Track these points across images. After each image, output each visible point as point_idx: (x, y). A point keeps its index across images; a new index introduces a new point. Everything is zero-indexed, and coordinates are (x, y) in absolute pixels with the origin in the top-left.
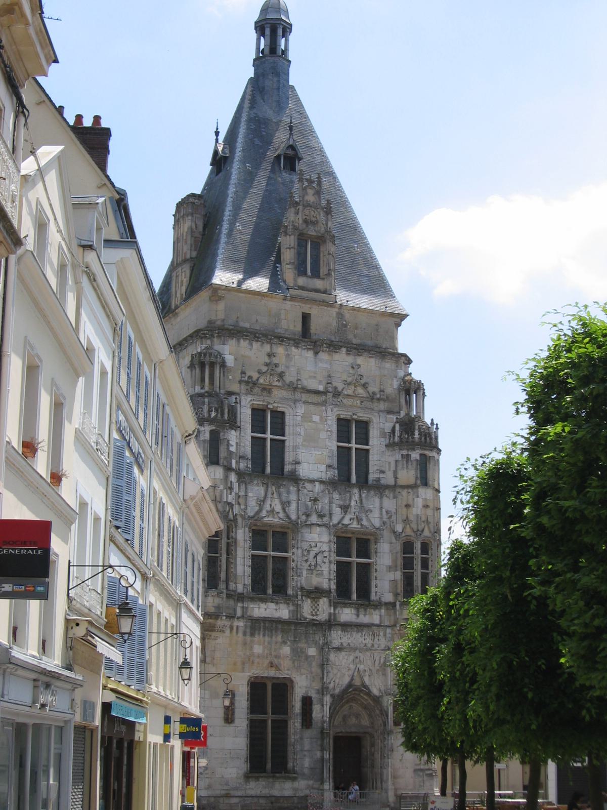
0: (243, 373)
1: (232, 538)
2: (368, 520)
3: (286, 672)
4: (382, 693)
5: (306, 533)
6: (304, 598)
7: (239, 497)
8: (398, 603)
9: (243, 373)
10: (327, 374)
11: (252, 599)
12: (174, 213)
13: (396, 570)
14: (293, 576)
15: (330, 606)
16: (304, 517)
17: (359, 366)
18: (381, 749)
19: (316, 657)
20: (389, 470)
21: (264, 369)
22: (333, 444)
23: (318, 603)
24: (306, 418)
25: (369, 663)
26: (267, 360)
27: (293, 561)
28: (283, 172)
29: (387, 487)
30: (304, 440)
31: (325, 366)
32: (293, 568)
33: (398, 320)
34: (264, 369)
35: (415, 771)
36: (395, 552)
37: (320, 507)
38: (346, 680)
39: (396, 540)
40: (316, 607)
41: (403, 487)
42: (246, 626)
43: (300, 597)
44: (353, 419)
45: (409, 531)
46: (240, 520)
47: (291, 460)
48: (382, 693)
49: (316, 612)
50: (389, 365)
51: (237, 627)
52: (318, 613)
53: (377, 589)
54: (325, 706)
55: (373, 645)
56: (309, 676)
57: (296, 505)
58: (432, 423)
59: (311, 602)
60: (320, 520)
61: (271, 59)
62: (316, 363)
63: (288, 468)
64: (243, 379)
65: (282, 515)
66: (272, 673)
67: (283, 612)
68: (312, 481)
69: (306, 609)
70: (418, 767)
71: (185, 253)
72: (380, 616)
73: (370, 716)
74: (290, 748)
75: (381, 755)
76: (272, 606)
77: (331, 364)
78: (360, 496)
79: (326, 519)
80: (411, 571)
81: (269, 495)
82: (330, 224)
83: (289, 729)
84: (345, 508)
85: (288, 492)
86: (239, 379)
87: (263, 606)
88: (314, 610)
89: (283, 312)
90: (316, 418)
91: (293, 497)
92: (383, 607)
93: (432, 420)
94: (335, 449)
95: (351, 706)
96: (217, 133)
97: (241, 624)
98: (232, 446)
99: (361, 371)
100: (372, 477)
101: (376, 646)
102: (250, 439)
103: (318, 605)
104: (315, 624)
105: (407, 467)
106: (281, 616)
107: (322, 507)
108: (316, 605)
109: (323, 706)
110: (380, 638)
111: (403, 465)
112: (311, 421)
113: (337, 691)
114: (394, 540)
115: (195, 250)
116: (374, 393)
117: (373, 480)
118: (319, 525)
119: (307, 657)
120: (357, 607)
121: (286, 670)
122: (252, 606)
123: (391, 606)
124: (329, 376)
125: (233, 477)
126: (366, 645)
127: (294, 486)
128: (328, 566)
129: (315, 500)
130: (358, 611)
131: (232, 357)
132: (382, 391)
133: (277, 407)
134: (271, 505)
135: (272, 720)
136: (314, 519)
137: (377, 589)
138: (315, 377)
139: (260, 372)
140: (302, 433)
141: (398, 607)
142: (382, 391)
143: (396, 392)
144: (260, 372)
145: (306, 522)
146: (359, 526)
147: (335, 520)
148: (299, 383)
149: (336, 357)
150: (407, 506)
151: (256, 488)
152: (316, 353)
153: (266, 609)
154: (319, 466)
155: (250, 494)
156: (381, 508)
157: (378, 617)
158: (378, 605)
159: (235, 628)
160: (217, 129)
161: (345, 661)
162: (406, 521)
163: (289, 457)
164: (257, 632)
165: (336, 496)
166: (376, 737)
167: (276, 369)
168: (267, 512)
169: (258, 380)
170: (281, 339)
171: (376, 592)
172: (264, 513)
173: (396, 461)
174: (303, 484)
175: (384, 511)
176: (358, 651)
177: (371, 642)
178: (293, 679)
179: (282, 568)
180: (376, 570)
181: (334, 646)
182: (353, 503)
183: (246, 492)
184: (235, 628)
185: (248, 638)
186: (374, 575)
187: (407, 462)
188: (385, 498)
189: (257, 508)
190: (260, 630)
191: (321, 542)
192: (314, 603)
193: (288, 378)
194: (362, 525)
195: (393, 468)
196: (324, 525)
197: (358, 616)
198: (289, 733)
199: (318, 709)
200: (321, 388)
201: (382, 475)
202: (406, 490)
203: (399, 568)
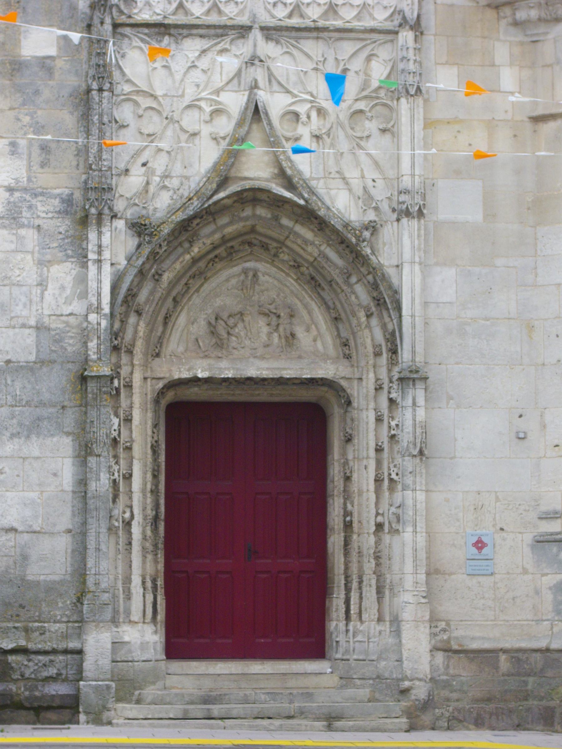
4: (376, 209)
18: (379, 450)
19: (60, 63)
48: (376, 209)
54: (92, 269)
56: (22, 143)
75: (378, 481)
95: (245, 272)
109: (84, 265)
161: (196, 76)
176: (256, 34)
181: (145, 16)
199: (68, 281)
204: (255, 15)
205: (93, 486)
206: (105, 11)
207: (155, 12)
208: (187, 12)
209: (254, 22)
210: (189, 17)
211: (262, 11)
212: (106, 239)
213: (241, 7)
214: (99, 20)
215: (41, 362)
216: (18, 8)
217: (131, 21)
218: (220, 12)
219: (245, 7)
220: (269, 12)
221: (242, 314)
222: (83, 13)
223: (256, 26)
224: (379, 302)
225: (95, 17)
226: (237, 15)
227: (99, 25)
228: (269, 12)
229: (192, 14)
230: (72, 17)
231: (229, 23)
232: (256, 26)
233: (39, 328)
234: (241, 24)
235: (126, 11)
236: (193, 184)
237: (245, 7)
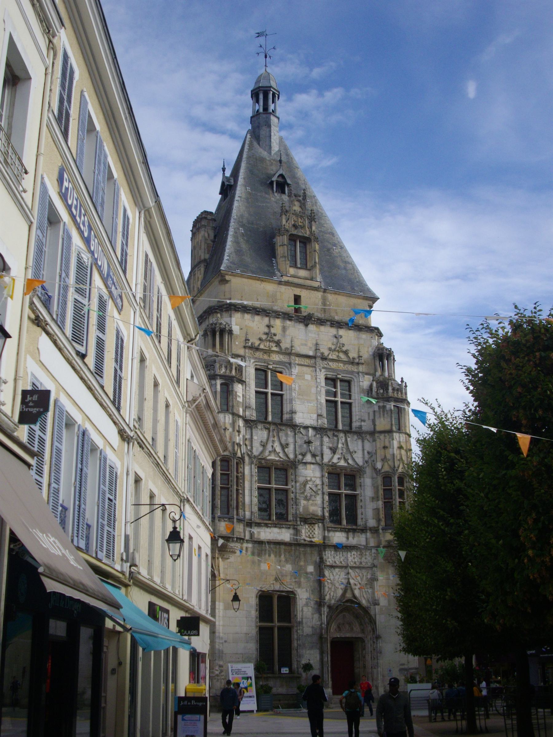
0: (247, 340)
1: (241, 472)
2: (354, 460)
3: (289, 586)
6: (302, 524)
7: (246, 439)
8: (380, 527)
9: (247, 340)
10: (315, 342)
11: (258, 525)
12: (191, 229)
13: (378, 500)
16: (300, 457)
17: (341, 337)
20: (369, 419)
21: (264, 337)
22: (323, 399)
24: (300, 376)
25: (359, 578)
26: (266, 330)
27: (293, 493)
28: (276, 194)
29: (367, 433)
30: (299, 395)
31: (313, 335)
32: (292, 499)
33: (371, 303)
34: (264, 337)
35: (401, 670)
36: (376, 485)
38: (340, 592)
39: (377, 475)
41: (381, 432)
42: (254, 547)
43: (299, 523)
44: (338, 378)
45: (386, 468)
46: (247, 459)
47: (288, 410)
50: (364, 336)
51: (247, 548)
52: (315, 536)
53: (363, 516)
55: (361, 563)
58: (402, 381)
59: (309, 527)
60: (314, 459)
61: (264, 116)
62: (306, 333)
63: (286, 417)
64: (247, 344)
65: (281, 455)
66: (277, 587)
67: (285, 535)
68: (306, 428)
69: (305, 533)
70: (403, 667)
71: (200, 256)
72: (366, 539)
73: (361, 624)
74: (294, 652)
75: (371, 658)
76: (276, 530)
77: (318, 335)
78: (346, 440)
79: (318, 458)
80: (390, 500)
81: (271, 439)
82: (314, 228)
83: (292, 636)
84: (334, 450)
85: (287, 435)
86: (244, 345)
87: (268, 530)
89: (278, 294)
90: (308, 377)
91: (291, 440)
92: (368, 531)
93: (402, 378)
94: (323, 402)
95: (344, 615)
96: (224, 170)
97: (250, 545)
98: (239, 397)
99: (342, 341)
100: (355, 425)
101: (364, 564)
102: (254, 393)
104: (312, 545)
105: (384, 415)
107: (315, 448)
108: (312, 529)
109: (321, 615)
110: (367, 557)
111: (380, 413)
112: (304, 379)
113: (333, 602)
114: (375, 475)
115: (208, 253)
116: (354, 358)
117: (356, 428)
118: (313, 464)
119: (307, 573)
120: (347, 531)
121: (288, 585)
122: (259, 530)
123: (375, 531)
124: (317, 344)
125: (241, 423)
126: (355, 563)
127: (291, 432)
129: (309, 443)
130: (348, 535)
131: (238, 327)
132: (360, 357)
133: (276, 367)
134: (272, 446)
135: (278, 628)
136: (309, 458)
137: (363, 516)
138: (306, 345)
139: (260, 339)
140: (297, 388)
141: (381, 531)
142: (360, 357)
143: (372, 357)
144: (260, 339)
146: (346, 464)
147: (326, 460)
148: (293, 348)
149: (322, 328)
150: (385, 447)
151: (260, 432)
152: (306, 325)
153: (270, 533)
154: (312, 415)
155: (255, 438)
156: (363, 450)
157: (364, 539)
158: (363, 530)
159: (244, 549)
160: (224, 166)
162: (384, 460)
163: (286, 408)
164: (263, 552)
165: (326, 439)
166: (366, 642)
167: (274, 337)
168: (270, 452)
169: (259, 345)
170: (277, 314)
171: (362, 519)
172: (267, 453)
173: (374, 412)
174: (299, 429)
175: (366, 452)
177: (359, 560)
178: (295, 592)
179: (283, 503)
180: (361, 500)
182: (340, 446)
183: (252, 435)
184: (244, 549)
185: (256, 558)
186: (359, 504)
187: (384, 411)
188: (366, 441)
189: (261, 449)
190: (266, 550)
191: (315, 477)
192: (311, 527)
193: (284, 345)
194: (348, 463)
195: (371, 417)
196: (316, 463)
197: (348, 538)
198: (292, 639)
199: (317, 618)
200: (311, 353)
201: (363, 423)
202: (383, 435)
203: (380, 499)
205: (324, 660)
212: (325, 609)
215: (313, 634)
221: (344, 624)
224: (371, 622)
233: (313, 627)
236: (338, 598)
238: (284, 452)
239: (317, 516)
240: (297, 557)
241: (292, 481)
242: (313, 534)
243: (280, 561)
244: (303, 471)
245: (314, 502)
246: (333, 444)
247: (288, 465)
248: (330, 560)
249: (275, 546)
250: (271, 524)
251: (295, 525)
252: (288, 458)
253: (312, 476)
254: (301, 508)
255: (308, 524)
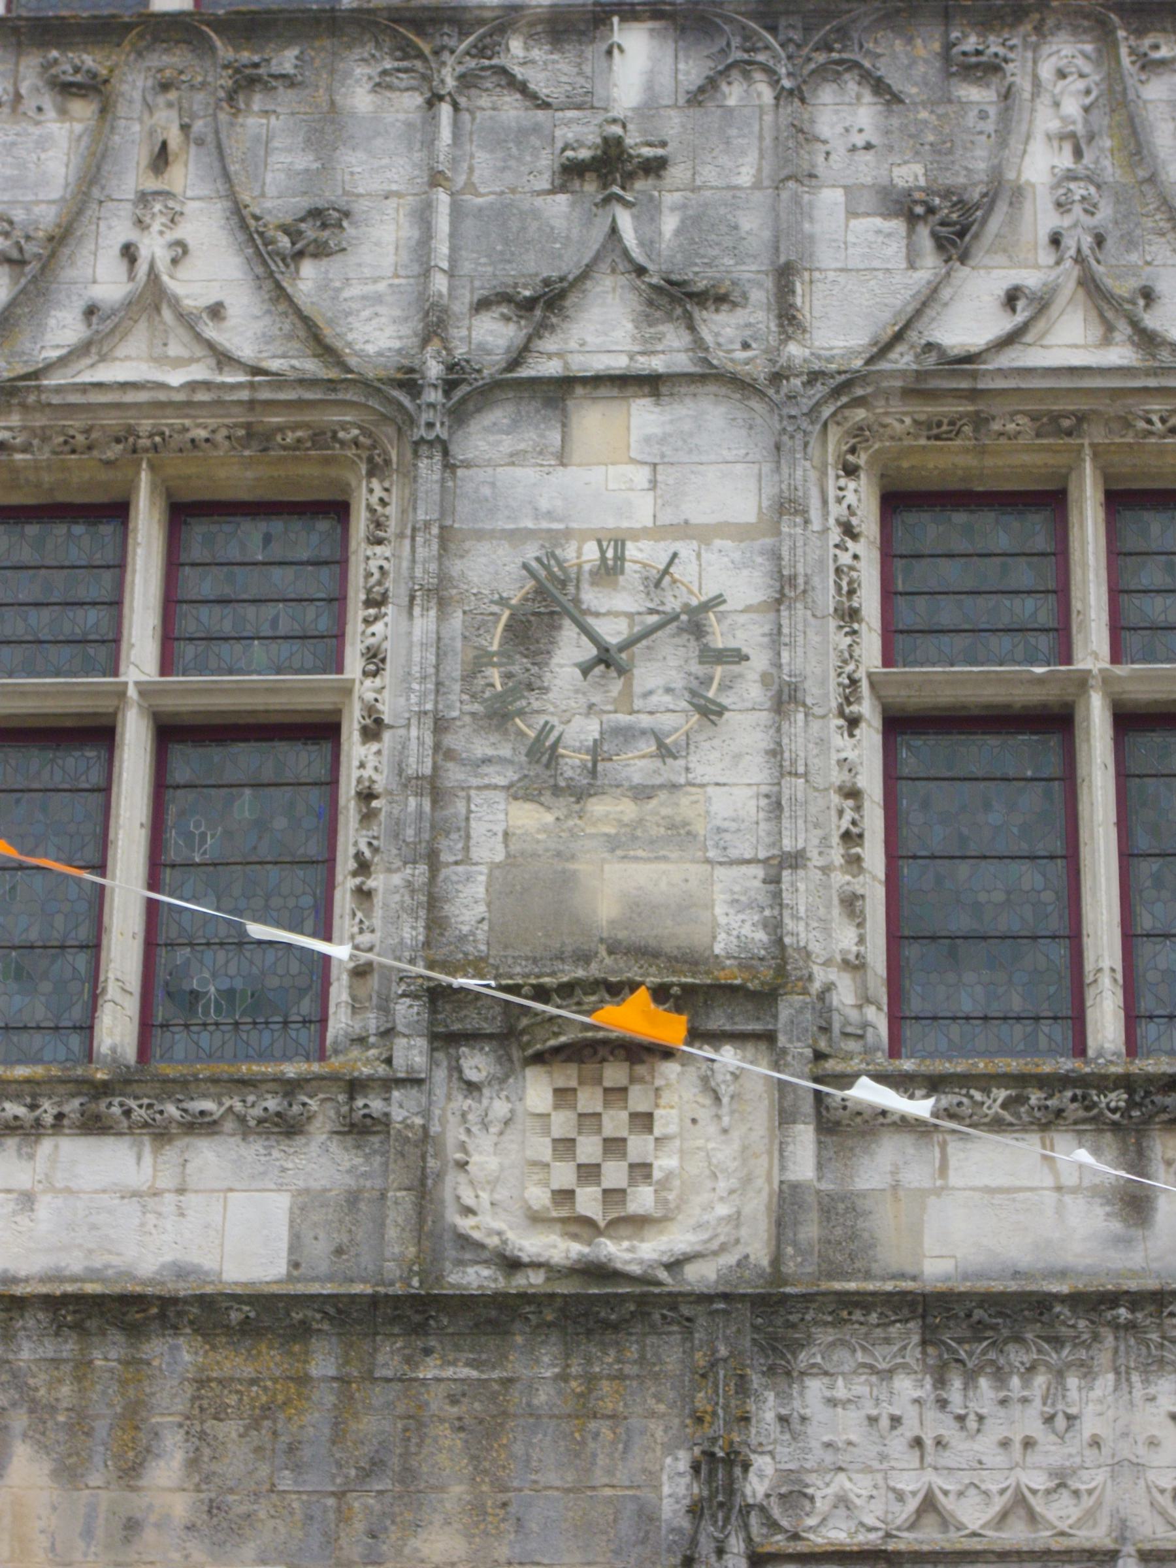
5: (516, 457)
14: (363, 867)
15: (785, 1117)
23: (638, 1100)
27: (373, 730)
37: (669, 224)
40: (614, 1146)
49: (613, 1196)
52: (642, 1199)
57: (409, 232)
59: (563, 1096)
88: (589, 1173)
103: (644, 1121)
106: (208, 1262)
108: (615, 1122)
128: (760, 740)
134: (129, 253)
145: (515, 363)
146: (1121, 354)
153: (27, 1200)
174: (481, 50)
191: (684, 530)
192: (589, 1100)
204: (1123, 1522)
206: (727, 1520)
207: (862, 1524)
208: (945, 1522)
209: (1122, 1539)
210: (953, 1534)
211: (1145, 1512)
213: (1087, 1502)
214: (713, 1545)
216: (504, 1520)
217: (800, 1547)
218: (1033, 1518)
219: (1099, 1504)
220: (1163, 1513)
222: (672, 1530)
223: (1129, 1549)
225: (703, 1539)
226: (1080, 1523)
227: (713, 1558)
228: (1163, 1513)
229: (960, 1527)
230: (643, 1542)
231: (1057, 1544)
232: (1129, 1549)
234: (1087, 1545)
235: (784, 1523)
237: (1099, 1504)
238: (280, 295)
239: (690, 960)
240: (374, 1467)
241: (376, 601)
242: (614, 1174)
243: (132, 1526)
244: (526, 474)
245: (659, 806)
246: (943, 150)
247: (322, 438)
248: (857, 1486)
249: (69, 1347)
250: (31, 1092)
251: (355, 1086)
252: (325, 350)
253: (643, 512)
254: (478, 889)
255: (539, 1059)
